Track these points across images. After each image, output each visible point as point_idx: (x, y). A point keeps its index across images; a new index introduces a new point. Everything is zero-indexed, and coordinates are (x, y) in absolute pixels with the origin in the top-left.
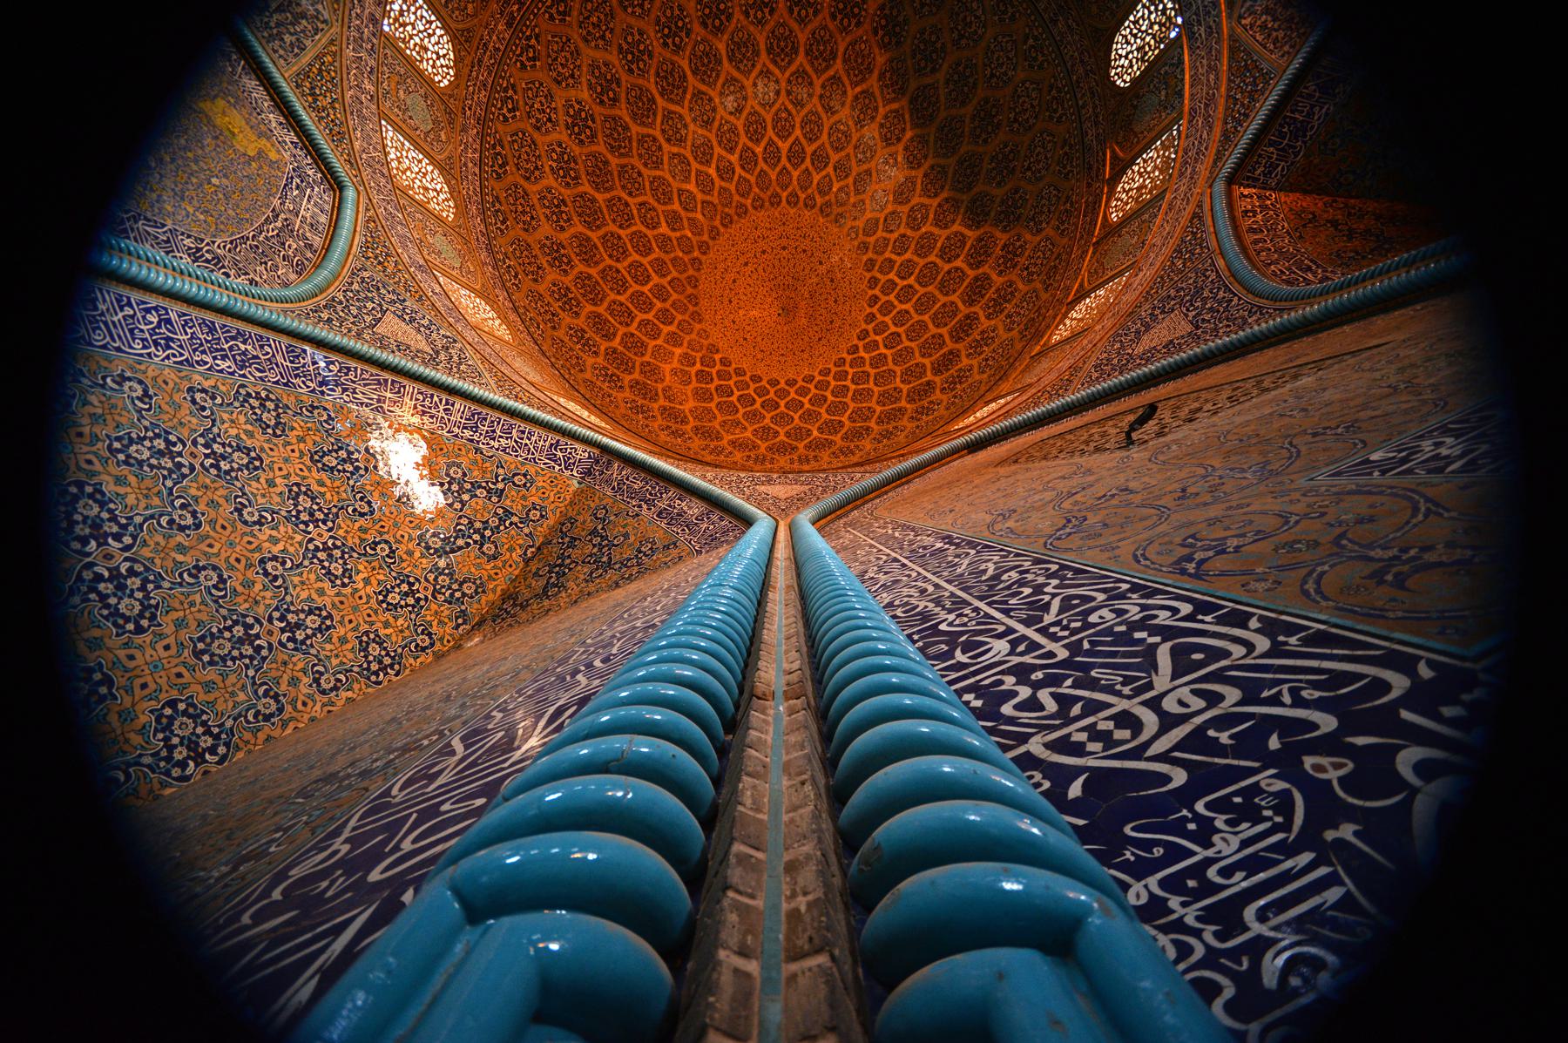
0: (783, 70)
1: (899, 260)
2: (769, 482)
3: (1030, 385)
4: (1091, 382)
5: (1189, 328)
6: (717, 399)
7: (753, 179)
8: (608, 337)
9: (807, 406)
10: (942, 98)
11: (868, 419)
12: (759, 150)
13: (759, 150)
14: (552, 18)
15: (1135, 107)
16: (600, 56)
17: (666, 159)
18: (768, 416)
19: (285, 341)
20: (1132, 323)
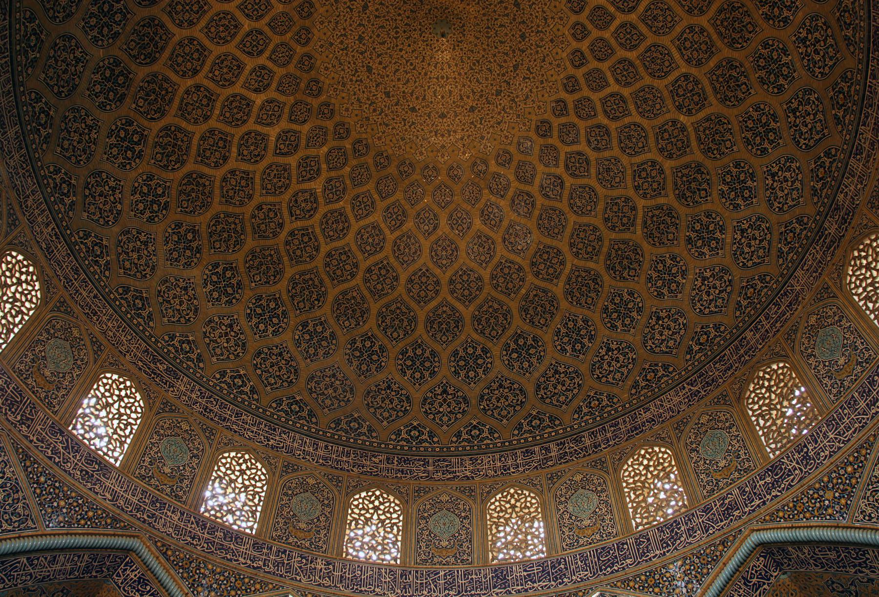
7: (276, 39)
9: (626, 92)
12: (247, 25)
13: (247, 25)
16: (162, 250)
17: (245, 167)
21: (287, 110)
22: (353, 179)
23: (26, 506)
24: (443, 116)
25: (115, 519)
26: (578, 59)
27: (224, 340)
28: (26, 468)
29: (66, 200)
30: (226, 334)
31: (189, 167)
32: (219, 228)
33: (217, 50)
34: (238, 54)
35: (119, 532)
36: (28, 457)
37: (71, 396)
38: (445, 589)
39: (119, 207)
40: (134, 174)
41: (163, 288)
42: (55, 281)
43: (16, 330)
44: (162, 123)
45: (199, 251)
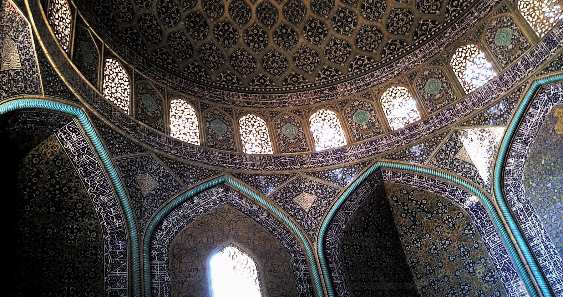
16: (281, 49)
23: (331, 188)
25: (363, 164)
27: (338, 52)
28: (318, 177)
29: (234, 81)
30: (337, 49)
31: (254, 8)
32: (290, 13)
35: (369, 166)
36: (315, 173)
37: (307, 139)
38: (526, 70)
39: (250, 57)
40: (241, 39)
41: (297, 62)
42: (262, 110)
43: (269, 140)
45: (293, 31)
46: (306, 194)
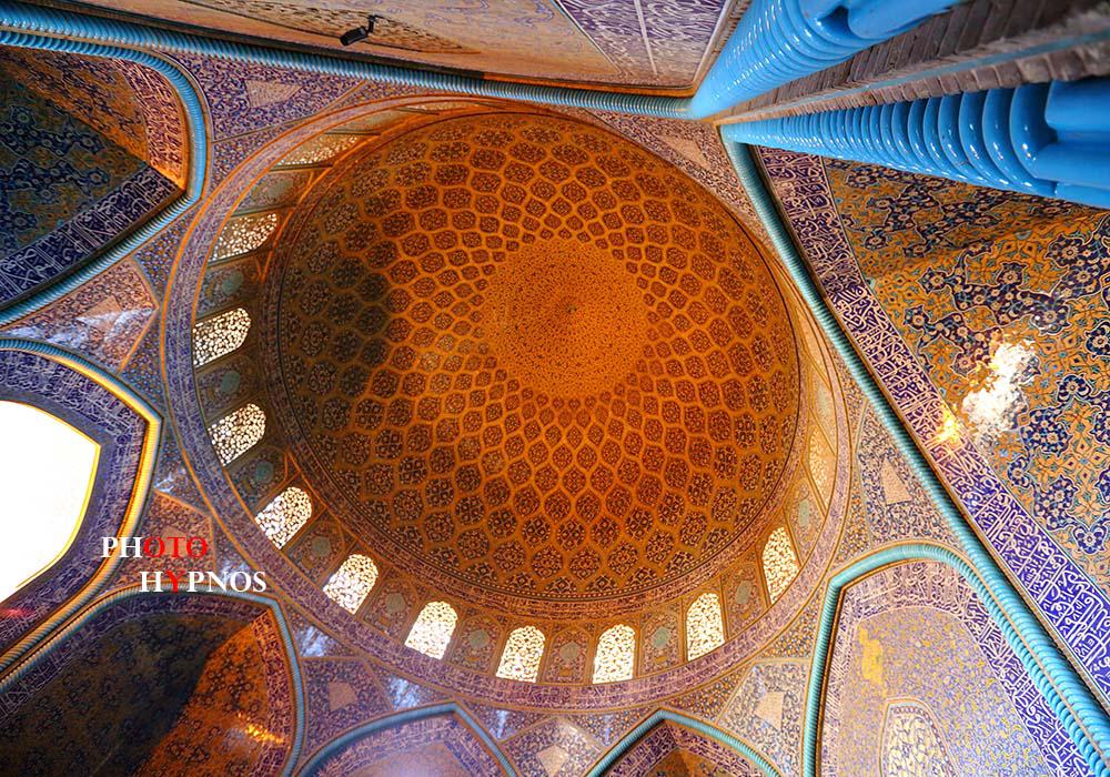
0: (475, 465)
1: (451, 289)
2: (693, 166)
3: (394, 108)
4: (345, 81)
5: (249, 84)
6: (681, 273)
7: (536, 417)
8: (736, 384)
9: (601, 213)
10: (371, 381)
11: (551, 164)
12: (520, 432)
13: (520, 432)
14: (613, 583)
15: (238, 291)
16: (596, 547)
17: (593, 469)
18: (643, 227)
19: (982, 534)
20: (289, 118)
21: (579, 427)
22: (633, 404)
24: (619, 328)
25: (641, 710)
26: (583, 237)
31: (573, 502)
33: (525, 455)
34: (533, 443)
44: (542, 504)
45: (614, 525)
46: (557, 748)
